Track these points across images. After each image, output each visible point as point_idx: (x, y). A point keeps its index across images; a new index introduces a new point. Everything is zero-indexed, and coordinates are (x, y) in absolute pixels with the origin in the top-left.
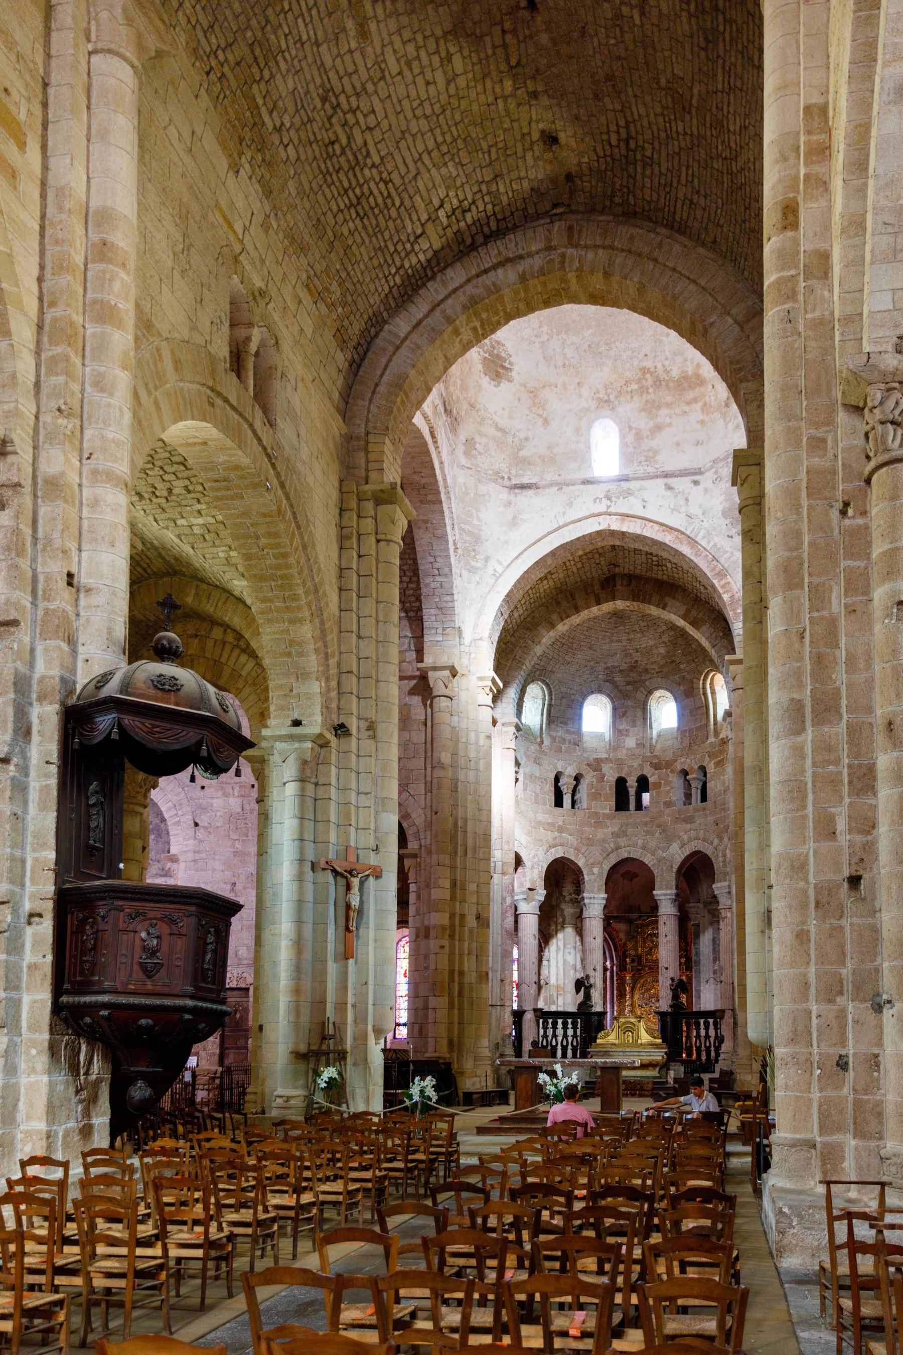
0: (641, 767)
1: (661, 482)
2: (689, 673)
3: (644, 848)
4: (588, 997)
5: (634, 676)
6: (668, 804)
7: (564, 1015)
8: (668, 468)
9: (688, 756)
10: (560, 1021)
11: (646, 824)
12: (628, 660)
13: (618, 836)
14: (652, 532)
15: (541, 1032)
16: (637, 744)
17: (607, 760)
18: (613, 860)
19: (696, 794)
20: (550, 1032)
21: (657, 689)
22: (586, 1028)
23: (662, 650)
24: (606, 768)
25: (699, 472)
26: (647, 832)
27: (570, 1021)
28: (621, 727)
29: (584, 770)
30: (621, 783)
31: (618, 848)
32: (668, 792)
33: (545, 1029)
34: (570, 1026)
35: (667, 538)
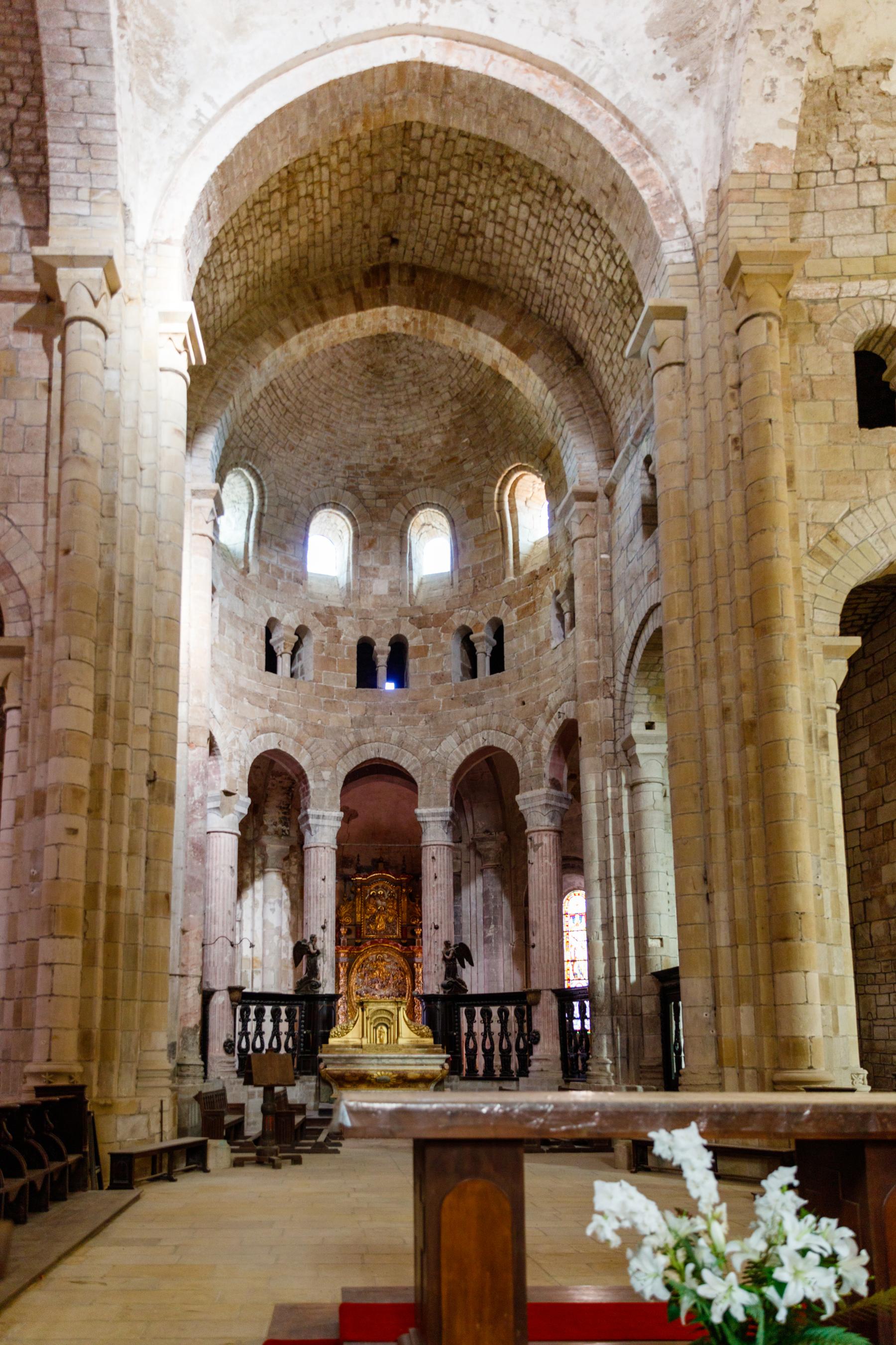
0: (397, 623)
2: (476, 476)
3: (401, 743)
4: (313, 970)
5: (389, 483)
6: (439, 679)
9: (470, 606)
10: (268, 1009)
11: (404, 708)
12: (382, 455)
13: (361, 725)
15: (239, 1025)
16: (391, 590)
17: (345, 611)
20: (252, 1026)
21: (424, 506)
22: (310, 1020)
23: (437, 440)
24: (343, 623)
26: (406, 721)
27: (283, 1009)
28: (366, 564)
29: (311, 622)
31: (360, 743)
32: (438, 661)
33: (245, 1021)
34: (283, 1016)
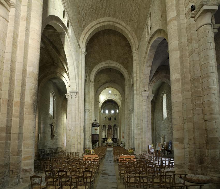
1: (114, 95)
7: (104, 138)
8: (115, 94)
14: (113, 99)
18: (108, 125)
19: (115, 119)
25: (117, 95)
30: (109, 118)
35: (114, 100)
